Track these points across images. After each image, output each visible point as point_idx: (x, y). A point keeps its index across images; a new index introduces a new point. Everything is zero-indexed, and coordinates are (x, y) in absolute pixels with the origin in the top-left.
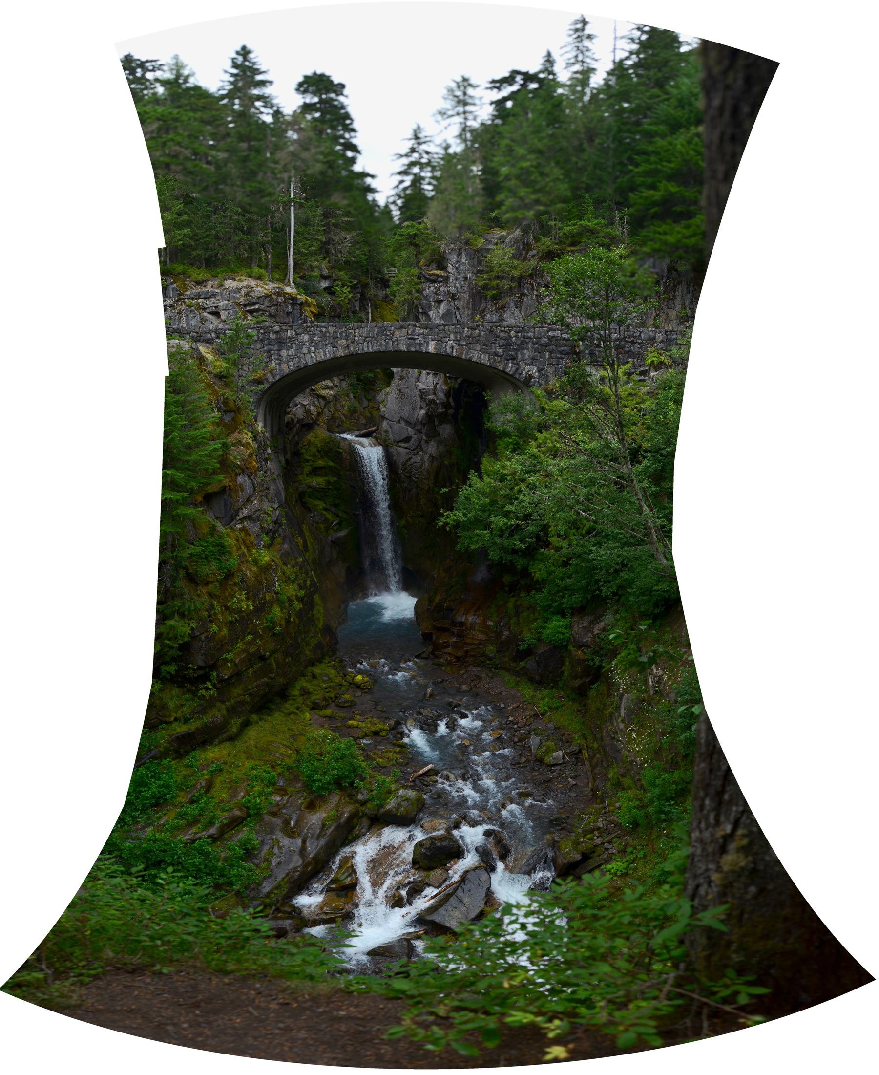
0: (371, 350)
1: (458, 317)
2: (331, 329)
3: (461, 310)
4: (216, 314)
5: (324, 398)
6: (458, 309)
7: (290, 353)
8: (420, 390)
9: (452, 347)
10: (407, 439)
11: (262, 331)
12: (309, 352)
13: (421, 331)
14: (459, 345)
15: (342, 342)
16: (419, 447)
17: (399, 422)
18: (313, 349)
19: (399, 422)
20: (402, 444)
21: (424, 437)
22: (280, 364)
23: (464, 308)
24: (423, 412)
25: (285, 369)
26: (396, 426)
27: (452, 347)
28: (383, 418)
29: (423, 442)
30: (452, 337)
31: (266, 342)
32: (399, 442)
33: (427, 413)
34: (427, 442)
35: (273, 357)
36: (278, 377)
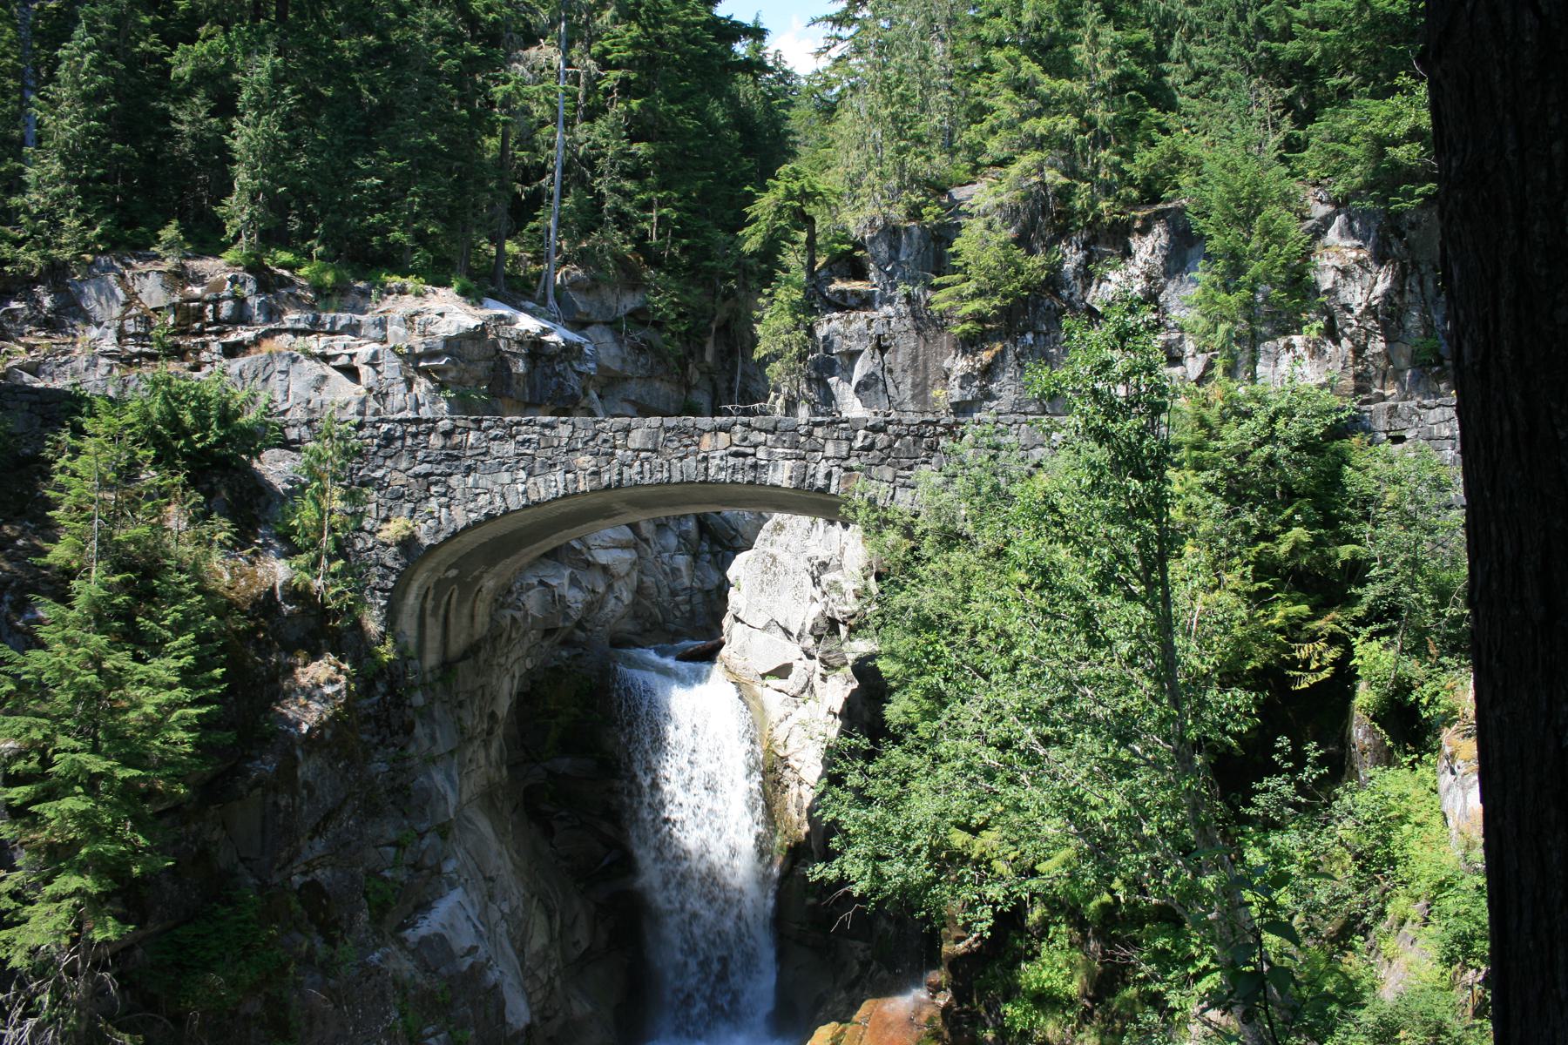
0: (647, 481)
1: (891, 390)
2: (564, 431)
3: (898, 372)
4: (351, 373)
5: (605, 569)
6: (890, 371)
7: (470, 480)
8: (810, 560)
9: (829, 475)
10: (783, 671)
11: (413, 429)
12: (514, 481)
13: (762, 437)
14: (846, 469)
15: (584, 461)
16: (808, 687)
17: (766, 628)
18: (522, 475)
19: (766, 628)
20: (776, 683)
21: (820, 669)
22: (448, 507)
23: (904, 371)
24: (817, 609)
25: (460, 518)
26: (760, 638)
27: (829, 475)
28: (737, 619)
29: (817, 679)
30: (830, 449)
31: (421, 455)
32: (763, 676)
33: (823, 614)
34: (824, 678)
35: (433, 489)
36: (441, 537)
